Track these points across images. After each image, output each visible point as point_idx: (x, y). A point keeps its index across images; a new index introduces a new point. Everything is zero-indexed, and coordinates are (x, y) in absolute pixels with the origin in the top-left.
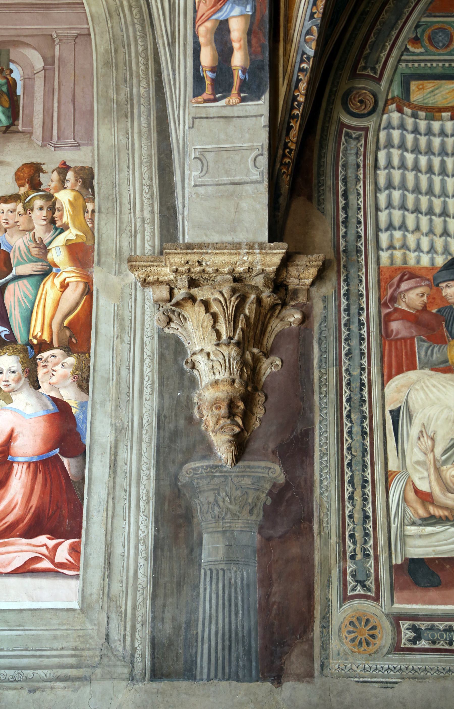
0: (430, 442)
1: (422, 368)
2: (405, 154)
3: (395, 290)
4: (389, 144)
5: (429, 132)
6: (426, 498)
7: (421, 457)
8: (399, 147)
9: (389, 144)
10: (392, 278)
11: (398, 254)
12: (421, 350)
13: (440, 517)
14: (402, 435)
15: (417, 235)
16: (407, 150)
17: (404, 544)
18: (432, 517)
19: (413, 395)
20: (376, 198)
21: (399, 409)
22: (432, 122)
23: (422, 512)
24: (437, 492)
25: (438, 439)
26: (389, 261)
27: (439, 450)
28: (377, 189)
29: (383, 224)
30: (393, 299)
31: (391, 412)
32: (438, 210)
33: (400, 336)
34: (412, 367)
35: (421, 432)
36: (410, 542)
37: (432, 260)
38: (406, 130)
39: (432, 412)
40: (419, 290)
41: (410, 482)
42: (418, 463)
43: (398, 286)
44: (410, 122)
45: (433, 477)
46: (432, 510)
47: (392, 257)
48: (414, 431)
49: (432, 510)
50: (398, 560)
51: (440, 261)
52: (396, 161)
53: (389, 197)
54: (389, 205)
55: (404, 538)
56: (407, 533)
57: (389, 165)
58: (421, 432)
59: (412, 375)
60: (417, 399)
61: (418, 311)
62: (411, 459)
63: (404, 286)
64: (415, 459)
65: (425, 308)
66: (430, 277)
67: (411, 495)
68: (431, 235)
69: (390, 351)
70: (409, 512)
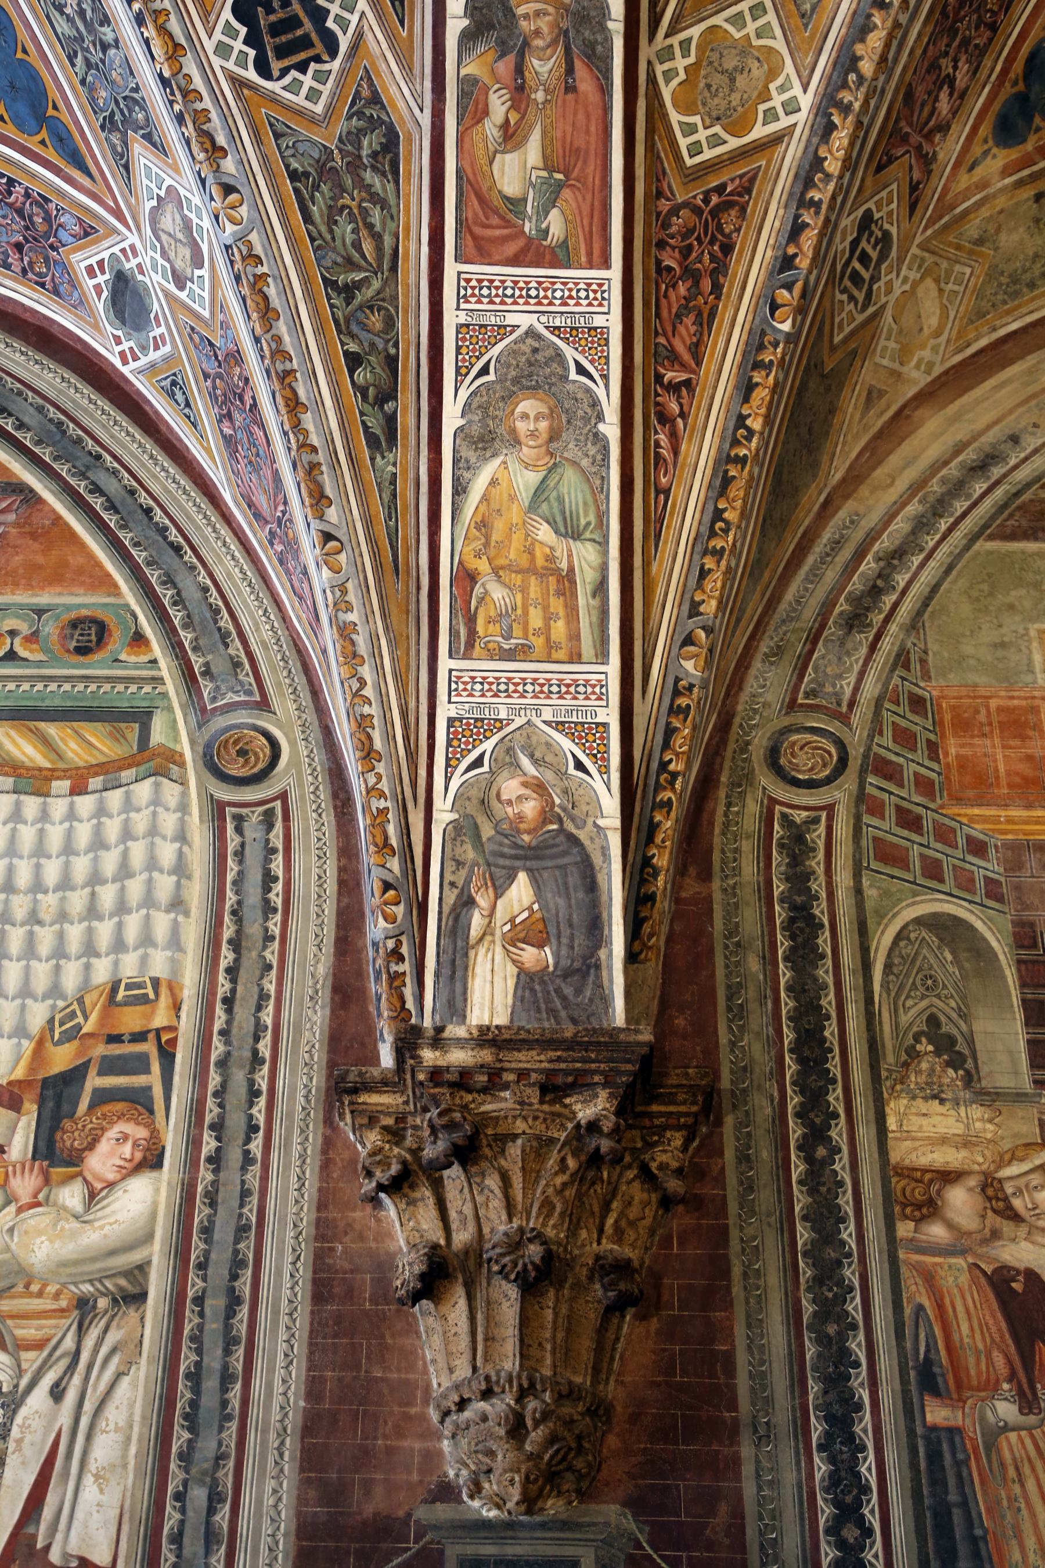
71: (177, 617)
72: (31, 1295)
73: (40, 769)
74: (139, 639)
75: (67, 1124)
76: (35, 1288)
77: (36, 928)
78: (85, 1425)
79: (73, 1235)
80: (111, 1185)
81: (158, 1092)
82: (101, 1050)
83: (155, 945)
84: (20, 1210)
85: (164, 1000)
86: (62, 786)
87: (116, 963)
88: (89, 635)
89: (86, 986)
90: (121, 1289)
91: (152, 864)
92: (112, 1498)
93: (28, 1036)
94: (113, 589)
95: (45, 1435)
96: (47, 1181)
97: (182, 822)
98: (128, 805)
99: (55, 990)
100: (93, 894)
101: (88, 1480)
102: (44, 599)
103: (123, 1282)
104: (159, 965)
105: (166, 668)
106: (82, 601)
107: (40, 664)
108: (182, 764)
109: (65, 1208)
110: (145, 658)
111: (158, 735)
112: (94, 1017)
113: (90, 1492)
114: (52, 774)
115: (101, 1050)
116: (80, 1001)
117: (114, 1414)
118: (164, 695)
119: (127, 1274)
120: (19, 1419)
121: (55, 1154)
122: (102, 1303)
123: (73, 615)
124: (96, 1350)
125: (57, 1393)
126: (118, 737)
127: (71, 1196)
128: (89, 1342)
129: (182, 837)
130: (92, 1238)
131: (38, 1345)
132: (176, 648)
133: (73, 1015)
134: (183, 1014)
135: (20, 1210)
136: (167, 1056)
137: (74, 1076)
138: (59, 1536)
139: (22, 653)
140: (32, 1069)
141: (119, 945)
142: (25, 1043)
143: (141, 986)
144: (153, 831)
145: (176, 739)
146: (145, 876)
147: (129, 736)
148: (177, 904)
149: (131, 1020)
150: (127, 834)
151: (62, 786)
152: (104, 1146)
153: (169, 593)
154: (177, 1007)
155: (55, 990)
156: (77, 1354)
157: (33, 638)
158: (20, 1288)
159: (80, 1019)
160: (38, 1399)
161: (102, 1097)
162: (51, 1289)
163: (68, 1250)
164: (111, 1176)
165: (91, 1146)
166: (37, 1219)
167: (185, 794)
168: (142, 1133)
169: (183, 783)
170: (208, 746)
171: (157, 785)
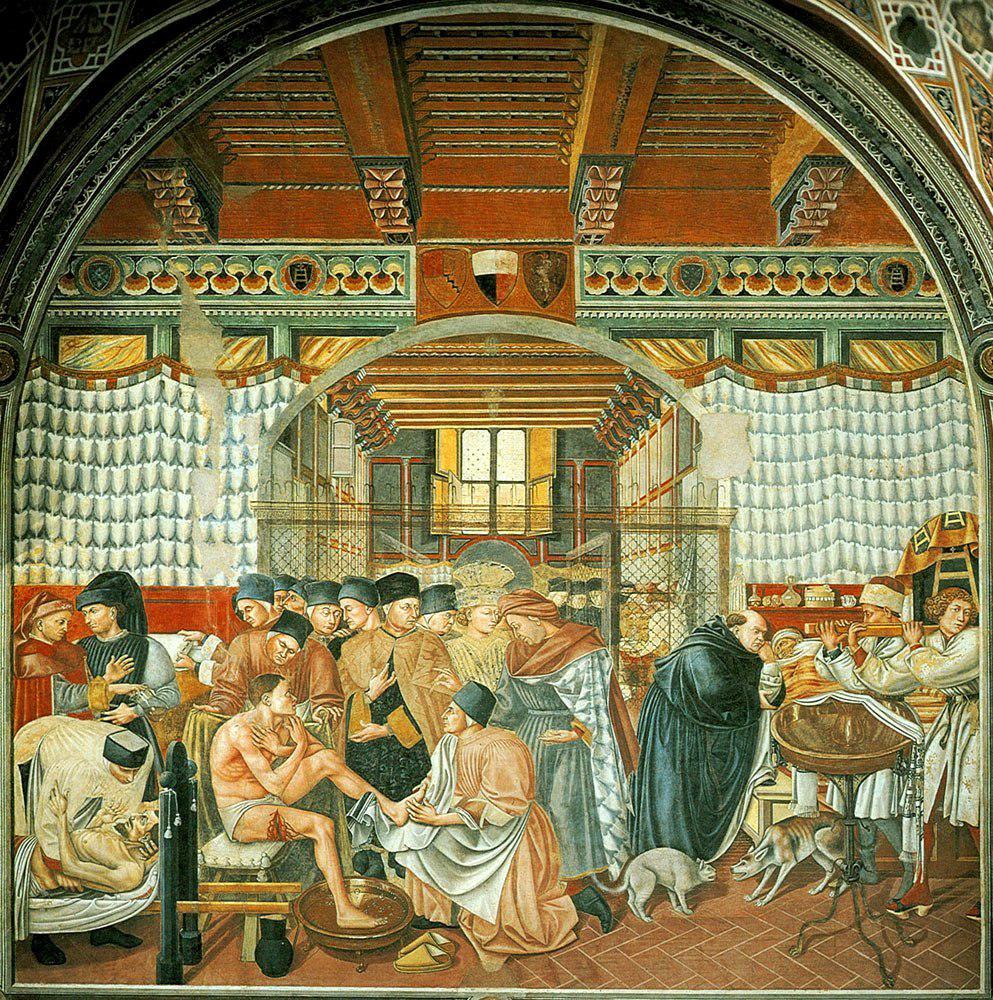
0: (62, 802)
1: (57, 713)
2: (50, 434)
3: (30, 616)
4: (31, 422)
5: (80, 406)
6: (54, 867)
7: (52, 820)
8: (43, 427)
9: (31, 422)
10: (27, 600)
11: (36, 569)
12: (56, 696)
13: (69, 888)
14: (32, 794)
15: (60, 542)
16: (52, 431)
17: (28, 919)
18: (62, 888)
19: (46, 748)
20: (13, 495)
21: (28, 764)
22: (83, 392)
23: (49, 882)
24: (68, 860)
25: (72, 797)
26: (25, 578)
27: (72, 811)
28: (14, 484)
29: (19, 532)
30: (28, 628)
31: (20, 766)
32: (85, 512)
33: (33, 674)
34: (46, 712)
35: (54, 790)
36: (35, 916)
37: (76, 576)
38: (53, 404)
39: (67, 766)
40: (58, 616)
41: (38, 847)
42: (47, 826)
43: (35, 611)
44: (57, 390)
45: (63, 843)
46: (61, 880)
47: (28, 574)
48: (46, 790)
49: (61, 880)
50: (21, 936)
51: (85, 578)
52: (38, 446)
53: (29, 492)
54: (28, 505)
55: (28, 911)
56: (32, 906)
57: (30, 451)
58: (54, 790)
59: (45, 720)
60: (50, 752)
61: (56, 642)
62: (40, 822)
63: (42, 610)
64: (44, 822)
65: (65, 636)
66: (72, 599)
67: (39, 864)
68: (75, 544)
69: (22, 693)
70: (36, 882)
71: (948, 261)
72: (923, 694)
73: (884, 374)
74: (928, 278)
75: (928, 600)
76: (925, 691)
77: (897, 481)
78: (959, 758)
79: (940, 663)
80: (955, 635)
81: (972, 580)
82: (941, 557)
83: (961, 492)
84: (912, 649)
85: (970, 527)
86: (897, 385)
87: (942, 503)
88: (900, 277)
89: (928, 519)
90: (967, 692)
91: (954, 440)
92: (975, 794)
93: (902, 549)
94: (913, 245)
95: (941, 765)
96: (923, 633)
97: (968, 410)
98: (937, 400)
99: (912, 521)
100: (925, 458)
101: (963, 787)
102: (869, 249)
103: (967, 688)
104: (965, 507)
105: (946, 300)
106: (892, 250)
107: (873, 298)
108: (963, 370)
109: (934, 648)
110: (933, 294)
111: (947, 351)
112: (934, 536)
113: (964, 792)
114: (891, 378)
115: (941, 557)
116: (926, 526)
117: (971, 755)
118: (948, 320)
119: (968, 684)
120: (927, 757)
121: (926, 619)
122: (959, 699)
123: (888, 261)
124: (958, 724)
125: (943, 745)
126: (924, 350)
127: (936, 641)
128: (955, 719)
129: (968, 421)
130: (950, 664)
131: (931, 721)
132: (949, 283)
133: (923, 536)
134: (980, 534)
135: (912, 649)
136: (975, 561)
137: (928, 574)
138: (953, 812)
139: (864, 291)
140: (906, 568)
141: (942, 492)
142: (901, 552)
143: (956, 517)
144: (952, 417)
145: (958, 353)
146: (951, 447)
147: (931, 350)
148: (970, 465)
149: (954, 540)
150: (938, 420)
151: (897, 385)
152: (949, 613)
153: (942, 243)
154: (976, 529)
155: (912, 521)
156: (950, 725)
157: (867, 278)
158: (918, 691)
159: (927, 538)
160: (935, 746)
161: (944, 585)
162: (933, 691)
163: (939, 671)
164: (954, 631)
165: (942, 614)
166: (920, 654)
167: (966, 390)
168: (967, 606)
169: (965, 383)
170: (976, 357)
171: (950, 384)
